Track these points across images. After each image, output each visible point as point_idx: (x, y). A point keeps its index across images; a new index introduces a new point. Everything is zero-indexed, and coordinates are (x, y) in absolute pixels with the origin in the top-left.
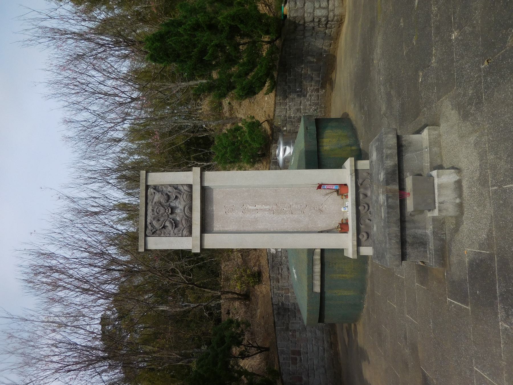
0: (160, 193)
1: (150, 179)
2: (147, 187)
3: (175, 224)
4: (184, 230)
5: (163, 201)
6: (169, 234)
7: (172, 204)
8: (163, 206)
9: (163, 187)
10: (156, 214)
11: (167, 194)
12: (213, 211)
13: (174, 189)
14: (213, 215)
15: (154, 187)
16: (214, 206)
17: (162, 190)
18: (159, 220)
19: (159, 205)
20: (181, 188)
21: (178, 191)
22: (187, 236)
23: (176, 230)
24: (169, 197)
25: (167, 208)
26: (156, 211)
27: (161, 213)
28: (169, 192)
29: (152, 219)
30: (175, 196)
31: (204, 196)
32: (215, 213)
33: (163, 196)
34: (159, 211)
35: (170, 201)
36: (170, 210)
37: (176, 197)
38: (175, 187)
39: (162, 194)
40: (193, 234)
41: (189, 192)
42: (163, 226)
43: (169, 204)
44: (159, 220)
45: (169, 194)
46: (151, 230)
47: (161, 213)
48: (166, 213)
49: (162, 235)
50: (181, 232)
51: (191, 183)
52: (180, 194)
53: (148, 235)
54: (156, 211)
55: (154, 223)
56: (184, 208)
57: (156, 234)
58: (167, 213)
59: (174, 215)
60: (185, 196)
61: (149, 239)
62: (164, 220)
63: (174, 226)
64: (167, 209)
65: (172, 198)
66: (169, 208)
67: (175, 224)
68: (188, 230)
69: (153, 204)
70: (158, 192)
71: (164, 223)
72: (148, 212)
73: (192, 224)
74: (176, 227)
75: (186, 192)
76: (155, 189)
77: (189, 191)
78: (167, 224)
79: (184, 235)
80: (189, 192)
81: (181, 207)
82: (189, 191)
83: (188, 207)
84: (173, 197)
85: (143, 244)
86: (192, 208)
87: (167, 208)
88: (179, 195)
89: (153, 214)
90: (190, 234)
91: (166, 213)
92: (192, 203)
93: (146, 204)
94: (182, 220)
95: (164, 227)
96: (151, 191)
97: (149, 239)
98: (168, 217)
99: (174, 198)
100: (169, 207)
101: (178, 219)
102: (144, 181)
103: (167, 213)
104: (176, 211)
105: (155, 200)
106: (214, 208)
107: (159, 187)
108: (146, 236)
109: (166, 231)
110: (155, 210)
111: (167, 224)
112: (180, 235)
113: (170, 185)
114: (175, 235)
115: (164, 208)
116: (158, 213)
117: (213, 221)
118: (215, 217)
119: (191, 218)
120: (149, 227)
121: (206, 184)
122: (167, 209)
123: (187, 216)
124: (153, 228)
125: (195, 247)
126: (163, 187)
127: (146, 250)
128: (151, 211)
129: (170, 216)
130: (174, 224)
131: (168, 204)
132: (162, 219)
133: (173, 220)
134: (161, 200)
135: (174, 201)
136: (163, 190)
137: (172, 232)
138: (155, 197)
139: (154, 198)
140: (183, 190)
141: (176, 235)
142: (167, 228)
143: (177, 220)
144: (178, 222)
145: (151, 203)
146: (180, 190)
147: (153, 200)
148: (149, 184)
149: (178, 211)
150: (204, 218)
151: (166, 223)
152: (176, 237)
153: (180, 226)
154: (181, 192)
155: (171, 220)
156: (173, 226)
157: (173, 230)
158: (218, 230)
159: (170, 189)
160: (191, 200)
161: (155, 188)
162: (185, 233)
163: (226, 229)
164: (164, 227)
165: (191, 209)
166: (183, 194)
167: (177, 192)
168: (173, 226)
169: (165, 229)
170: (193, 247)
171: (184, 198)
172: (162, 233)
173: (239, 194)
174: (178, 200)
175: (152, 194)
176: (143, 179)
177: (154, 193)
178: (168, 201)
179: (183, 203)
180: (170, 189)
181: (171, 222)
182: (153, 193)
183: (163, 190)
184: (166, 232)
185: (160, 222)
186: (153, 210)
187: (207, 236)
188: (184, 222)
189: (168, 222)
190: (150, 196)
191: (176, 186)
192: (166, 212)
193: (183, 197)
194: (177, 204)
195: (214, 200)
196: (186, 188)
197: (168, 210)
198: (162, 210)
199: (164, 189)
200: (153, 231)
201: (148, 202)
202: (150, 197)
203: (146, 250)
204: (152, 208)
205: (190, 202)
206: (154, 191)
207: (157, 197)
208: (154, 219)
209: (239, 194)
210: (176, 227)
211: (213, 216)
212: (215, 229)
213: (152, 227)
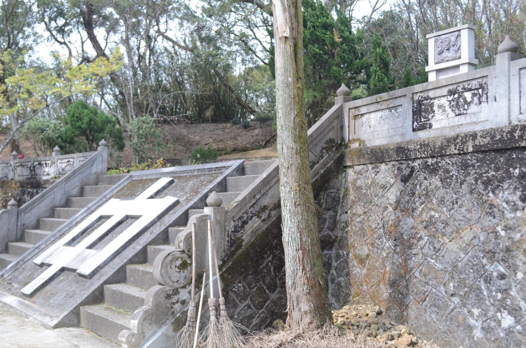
2: (459, 31)
3: (440, 53)
18: (442, 43)
24: (454, 46)
38: (459, 49)
44: (442, 43)
55: (440, 40)
67: (440, 53)
70: (457, 38)
76: (458, 36)
78: (440, 49)
90: (436, 63)
96: (456, 33)
114: (435, 54)
120: (439, 38)
121: (461, 67)
127: (428, 39)
132: (443, 44)
148: (462, 31)
149: (447, 53)
153: (439, 57)
159: (459, 45)
161: (459, 36)
162: (436, 60)
165: (448, 61)
180: (459, 45)
181: (441, 50)
185: (441, 44)
186: (446, 38)
187: (435, 73)
196: (458, 55)
198: (446, 44)
203: (428, 39)
207: (453, 39)
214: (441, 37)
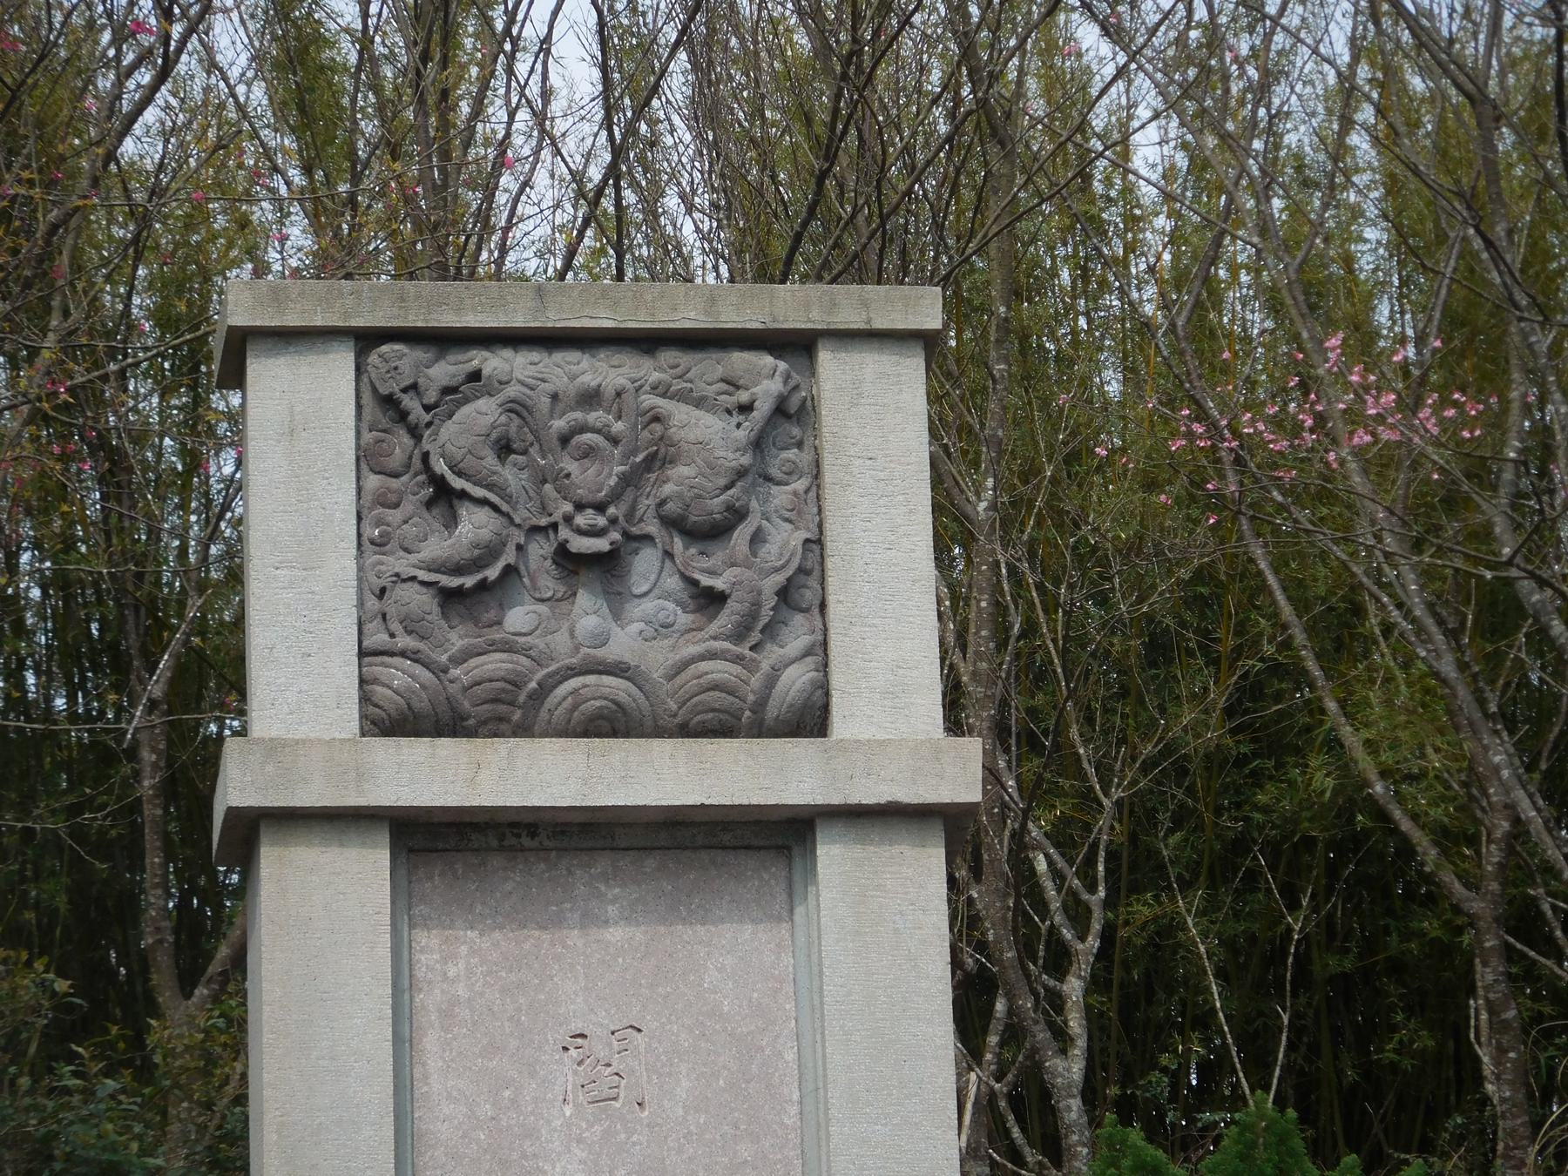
0: (746, 460)
1: (871, 364)
4: (419, 670)
5: (677, 482)
6: (380, 544)
7: (645, 563)
8: (629, 481)
9: (800, 485)
10: (559, 424)
11: (737, 514)
12: (590, 920)
13: (779, 579)
14: (557, 922)
15: (794, 405)
16: (638, 934)
17: (775, 472)
18: (504, 449)
19: (634, 452)
20: (797, 636)
21: (766, 614)
22: (365, 699)
23: (418, 600)
24: (711, 533)
25: (613, 521)
26: (583, 429)
27: (571, 466)
28: (757, 538)
29: (512, 391)
30: (719, 584)
31: (726, 838)
32: (574, 937)
33: (722, 482)
34: (588, 453)
35: (678, 544)
36: (601, 545)
37: (709, 600)
39: (741, 473)
40: (386, 750)
41: (760, 705)
42: (457, 483)
43: (648, 538)
44: (504, 449)
45: (741, 535)
46: (413, 387)
47: (571, 466)
48: (568, 507)
49: (373, 481)
50: (404, 641)
51: (841, 727)
52: (739, 635)
53: (373, 358)
54: (583, 429)
55: (482, 412)
56: (618, 669)
57: (385, 422)
58: (568, 519)
59: (549, 584)
60: (721, 670)
61: (341, 361)
62: (507, 498)
63: (454, 582)
64: (601, 521)
65: (706, 563)
66: (615, 536)
68: (422, 704)
69: (649, 400)
70: (758, 444)
71: (479, 492)
72: (572, 356)
73: (471, 733)
74: (449, 597)
75: (756, 681)
76: (781, 411)
77: (772, 711)
78: (474, 525)
79: (377, 669)
80: (760, 705)
81: (624, 643)
82: (772, 711)
83: (623, 697)
84: (712, 573)
85: (292, 320)
86: (614, 734)
87: (613, 521)
88: (725, 619)
89: (555, 397)
91: (568, 507)
92: (659, 732)
93: (648, 342)
94: (508, 647)
95: (444, 497)
97: (341, 361)
98: (535, 530)
99: (706, 581)
100: (627, 535)
101: (519, 617)
102: (850, 317)
103: (568, 519)
104: (584, 599)
105: (679, 413)
106: (615, 934)
107: (800, 445)
108: (367, 340)
109: (409, 518)
110: (596, 417)
111: (474, 525)
112: (378, 638)
113: (816, 544)
115: (615, 496)
116: (565, 440)
117: (501, 927)
118: (535, 940)
119: (524, 730)
120: (445, 370)
122: (601, 521)
123: (544, 689)
124: (431, 397)
125: (269, 768)
126: (800, 485)
128: (589, 380)
129: (539, 551)
130: (469, 581)
131: (652, 527)
132: (511, 476)
133: (510, 571)
134: (682, 471)
135: (672, 582)
136: (769, 479)
137: (401, 564)
138: (712, 409)
139: (699, 403)
140: (772, 655)
141: (372, 603)
142: (433, 520)
143: (503, 608)
144: (491, 615)
145: (656, 376)
146: (770, 631)
147: (683, 397)
148: (826, 358)
150: (526, 842)
151: (482, 515)
152: (361, 604)
153: (458, 639)
154: (755, 637)
155: (509, 557)
156: (458, 570)
157: (423, 575)
158: (420, 973)
160: (685, 731)
162: (399, 677)
163: (430, 1042)
164: (444, 497)
166: (738, 659)
167: (757, 605)
168: (458, 570)
169: (429, 504)
170: (274, 747)
171: (704, 666)
172: (395, 483)
173: (745, 1151)
174: (684, 619)
175: (733, 384)
176: (865, 304)
177: (746, 408)
178: (675, 524)
179: (657, 658)
180: (784, 541)
181: (490, 552)
182: (744, 397)
183: (769, 479)
184: (394, 516)
185: (491, 460)
186: (590, 398)
188: (495, 664)
189: (485, 534)
190: (720, 371)
191: (809, 596)
192: (580, 507)
193: (711, 656)
194: (648, 606)
195: (685, 932)
196: (796, 680)
197: (597, 533)
199: (780, 496)
200: (410, 402)
201: (668, 356)
202: (707, 368)
204: (609, 392)
205: (667, 721)
206: (763, 408)
208: (517, 408)
209: (745, 1151)
210: (449, 597)
211: (543, 928)
212: (429, 945)
213: (448, 390)
214: (493, 362)
